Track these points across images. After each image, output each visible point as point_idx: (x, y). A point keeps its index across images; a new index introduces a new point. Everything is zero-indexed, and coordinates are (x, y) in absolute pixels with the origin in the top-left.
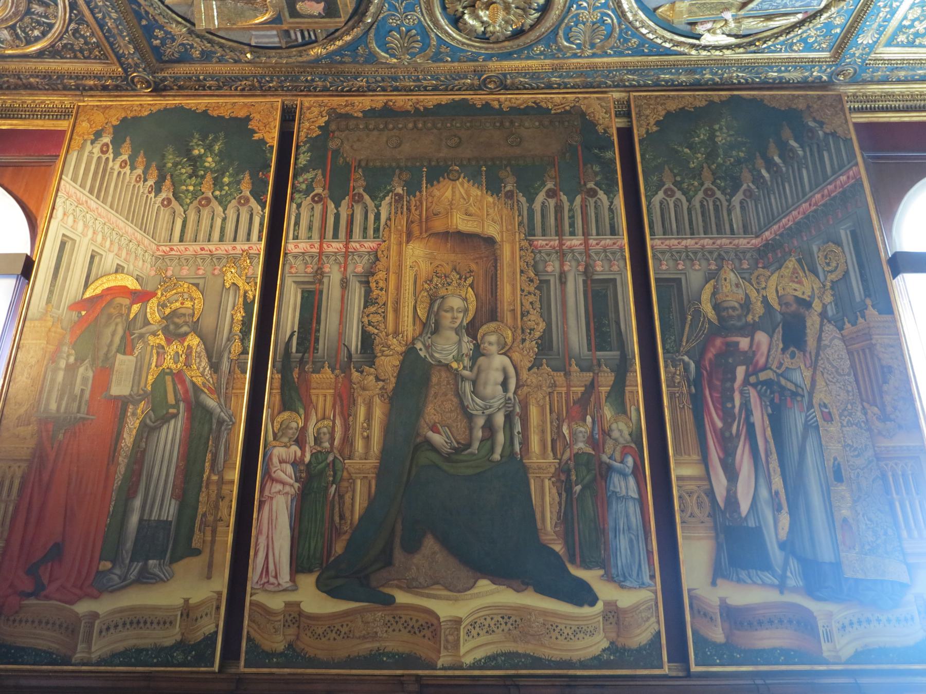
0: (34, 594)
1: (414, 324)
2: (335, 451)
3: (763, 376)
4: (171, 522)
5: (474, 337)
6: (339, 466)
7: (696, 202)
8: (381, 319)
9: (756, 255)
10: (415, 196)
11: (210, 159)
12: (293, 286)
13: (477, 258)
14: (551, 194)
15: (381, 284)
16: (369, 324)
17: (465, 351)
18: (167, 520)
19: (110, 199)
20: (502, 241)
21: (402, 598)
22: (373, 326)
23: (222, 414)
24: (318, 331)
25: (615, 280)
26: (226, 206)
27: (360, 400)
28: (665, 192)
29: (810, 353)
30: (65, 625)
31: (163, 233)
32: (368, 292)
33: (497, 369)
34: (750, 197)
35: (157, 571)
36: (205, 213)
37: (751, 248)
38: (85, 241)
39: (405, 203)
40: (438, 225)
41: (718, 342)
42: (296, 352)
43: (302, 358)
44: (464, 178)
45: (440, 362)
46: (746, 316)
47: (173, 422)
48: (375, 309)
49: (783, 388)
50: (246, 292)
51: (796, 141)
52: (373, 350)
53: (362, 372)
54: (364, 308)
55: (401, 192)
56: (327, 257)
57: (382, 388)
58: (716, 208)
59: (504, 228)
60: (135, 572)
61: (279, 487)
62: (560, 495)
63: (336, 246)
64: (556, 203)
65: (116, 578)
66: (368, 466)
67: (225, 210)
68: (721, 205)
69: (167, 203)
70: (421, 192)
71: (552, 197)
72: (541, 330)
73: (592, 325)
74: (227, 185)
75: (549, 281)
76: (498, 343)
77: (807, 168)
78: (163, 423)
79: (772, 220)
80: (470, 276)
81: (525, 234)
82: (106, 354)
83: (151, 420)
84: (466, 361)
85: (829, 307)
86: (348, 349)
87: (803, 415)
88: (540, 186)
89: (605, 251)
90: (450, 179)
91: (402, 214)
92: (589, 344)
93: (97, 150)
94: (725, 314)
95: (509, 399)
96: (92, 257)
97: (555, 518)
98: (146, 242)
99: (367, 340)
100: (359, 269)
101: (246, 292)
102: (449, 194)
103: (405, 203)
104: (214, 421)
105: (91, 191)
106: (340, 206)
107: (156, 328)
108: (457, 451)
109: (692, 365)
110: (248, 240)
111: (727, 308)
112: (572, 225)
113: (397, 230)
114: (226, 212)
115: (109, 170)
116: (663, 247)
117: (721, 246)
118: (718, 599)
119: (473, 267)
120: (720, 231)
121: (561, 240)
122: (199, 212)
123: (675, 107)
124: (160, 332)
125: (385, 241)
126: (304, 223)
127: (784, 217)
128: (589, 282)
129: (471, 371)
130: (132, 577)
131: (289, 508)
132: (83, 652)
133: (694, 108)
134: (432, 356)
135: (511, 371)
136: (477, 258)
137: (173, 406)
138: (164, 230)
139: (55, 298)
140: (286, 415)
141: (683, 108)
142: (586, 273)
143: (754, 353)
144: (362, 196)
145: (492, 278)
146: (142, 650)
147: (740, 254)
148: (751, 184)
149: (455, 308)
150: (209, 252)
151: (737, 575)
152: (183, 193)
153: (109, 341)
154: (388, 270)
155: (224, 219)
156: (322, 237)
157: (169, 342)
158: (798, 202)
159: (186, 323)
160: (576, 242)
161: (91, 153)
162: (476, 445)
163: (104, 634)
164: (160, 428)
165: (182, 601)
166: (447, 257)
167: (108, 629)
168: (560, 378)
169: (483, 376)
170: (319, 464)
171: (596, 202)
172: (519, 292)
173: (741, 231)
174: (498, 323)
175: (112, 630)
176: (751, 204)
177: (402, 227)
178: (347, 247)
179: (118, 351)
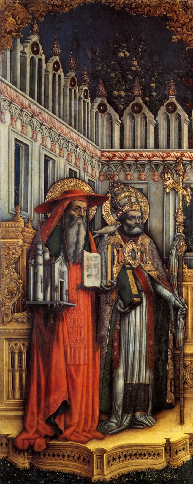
4: (148, 385)
11: (135, 63)
18: (145, 384)
23: (177, 302)
26: (157, 113)
30: (82, 457)
31: (105, 140)
35: (142, 419)
38: (37, 145)
47: (138, 308)
50: (184, 197)
60: (127, 421)
65: (114, 425)
67: (155, 115)
69: (102, 109)
78: (131, 309)
83: (121, 307)
93: (28, 50)
98: (91, 148)
104: (171, 307)
105: (32, 95)
107: (113, 229)
110: (180, 146)
114: (157, 119)
115: (44, 72)
122: (133, 118)
124: (117, 233)
132: (99, 475)
137: (137, 296)
138: (104, 136)
146: (140, 473)
150: (147, 159)
159: (137, 225)
161: (23, 52)
163: (111, 463)
164: (129, 313)
165: (164, 441)
167: (114, 459)
175: (117, 460)
179: (84, 248)
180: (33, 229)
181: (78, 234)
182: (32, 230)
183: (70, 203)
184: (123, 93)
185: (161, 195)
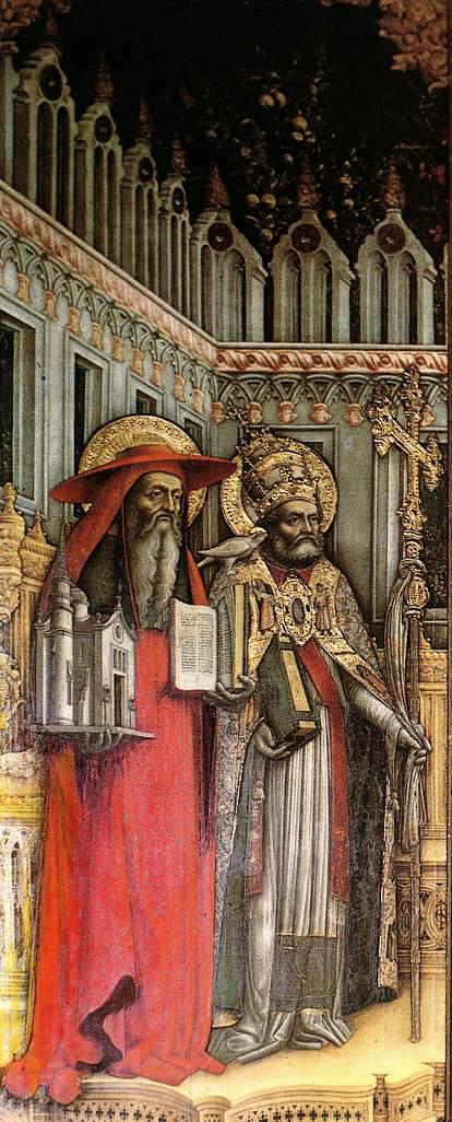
19: (90, 223)
31: (227, 319)
35: (320, 1027)
36: (311, 268)
38: (56, 331)
50: (421, 467)
65: (250, 1039)
67: (353, 259)
74: (350, 196)
78: (293, 749)
82: (152, 603)
83: (266, 741)
96: (80, 375)
104: (391, 746)
105: (43, 202)
110: (413, 337)
114: (357, 266)
115: (72, 144)
122: (297, 263)
124: (256, 555)
130: (280, 1039)
152: (254, 212)
153: (153, 572)
155: (355, 287)
157: (280, 578)
159: (307, 536)
165: (373, 1083)
179: (175, 594)
181: (159, 558)
182: (43, 545)
183: (138, 481)
184: (271, 201)
185: (369, 462)
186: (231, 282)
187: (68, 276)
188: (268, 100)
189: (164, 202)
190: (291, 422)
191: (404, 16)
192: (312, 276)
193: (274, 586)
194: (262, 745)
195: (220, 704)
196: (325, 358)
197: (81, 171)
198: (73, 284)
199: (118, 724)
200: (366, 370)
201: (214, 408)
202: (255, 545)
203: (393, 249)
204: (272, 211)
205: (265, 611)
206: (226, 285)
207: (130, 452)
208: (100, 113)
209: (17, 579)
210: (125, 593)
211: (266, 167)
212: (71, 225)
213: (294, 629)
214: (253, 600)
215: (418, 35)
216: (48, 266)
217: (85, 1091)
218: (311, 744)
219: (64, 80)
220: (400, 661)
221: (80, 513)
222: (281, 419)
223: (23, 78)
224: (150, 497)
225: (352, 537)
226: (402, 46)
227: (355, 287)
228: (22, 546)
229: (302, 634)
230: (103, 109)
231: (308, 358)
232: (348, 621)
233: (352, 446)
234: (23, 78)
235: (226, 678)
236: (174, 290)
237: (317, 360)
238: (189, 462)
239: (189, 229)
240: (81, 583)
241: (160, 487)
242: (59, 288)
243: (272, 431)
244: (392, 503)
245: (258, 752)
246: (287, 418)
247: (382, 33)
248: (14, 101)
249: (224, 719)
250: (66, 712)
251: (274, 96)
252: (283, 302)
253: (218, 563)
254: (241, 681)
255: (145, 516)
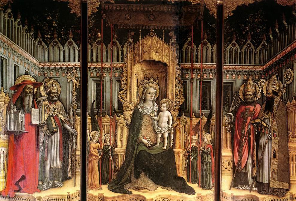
0: (18, 191)
1: (137, 99)
2: (111, 145)
3: (256, 121)
5: (159, 105)
6: (113, 150)
7: (243, 50)
8: (125, 96)
9: (262, 73)
10: (136, 43)
11: (54, 22)
12: (93, 82)
13: (160, 72)
14: (190, 44)
15: (125, 82)
16: (121, 98)
17: (155, 109)
20: (170, 65)
21: (134, 192)
22: (122, 99)
24: (103, 100)
25: (210, 82)
26: (64, 45)
27: (119, 127)
28: (232, 45)
29: (274, 112)
31: (41, 58)
32: (120, 85)
33: (166, 117)
34: (264, 48)
36: (56, 48)
37: (260, 70)
38: (11, 60)
39: (133, 46)
40: (146, 57)
41: (243, 108)
42: (96, 109)
43: (98, 111)
44: (156, 35)
45: (146, 113)
46: (254, 98)
48: (123, 92)
49: (262, 125)
50: (76, 84)
51: (286, 22)
52: (123, 108)
53: (119, 117)
54: (119, 92)
55: (131, 41)
56: (104, 70)
57: (126, 123)
58: (250, 52)
59: (170, 59)
61: (94, 157)
62: (186, 160)
63: (107, 65)
64: (191, 48)
66: (123, 150)
67: (64, 47)
68: (252, 51)
69: (40, 43)
70: (139, 41)
71: (190, 45)
72: (183, 102)
73: (201, 99)
75: (187, 81)
76: (167, 107)
77: (288, 35)
78: (53, 134)
79: (270, 58)
80: (158, 79)
81: (178, 62)
82: (28, 108)
83: (48, 133)
84: (156, 114)
85: (284, 95)
86: (114, 107)
87: (267, 135)
88: (185, 40)
89: (208, 69)
90: (150, 36)
91: (132, 51)
92: (199, 108)
94: (247, 97)
95: (170, 128)
96: (15, 67)
97: (184, 168)
99: (121, 104)
100: (117, 76)
101: (76, 84)
102: (150, 43)
103: (133, 46)
104: (70, 134)
106: (108, 47)
108: (152, 146)
109: (233, 116)
110: (74, 61)
111: (248, 95)
112: (197, 58)
113: (130, 59)
114: (64, 48)
115: (13, 26)
116: (228, 69)
117: (250, 69)
118: (231, 194)
119: (160, 76)
120: (250, 63)
121: (192, 64)
122: (54, 48)
123: (241, 4)
124: (46, 100)
125: (125, 63)
126: (94, 54)
127: (275, 57)
128: (201, 83)
129: (157, 117)
131: (98, 164)
133: (248, 4)
134: (144, 111)
135: (171, 118)
136: (160, 72)
139: (4, 84)
140: (94, 132)
141: (244, 4)
142: (200, 79)
143: (255, 112)
144: (116, 42)
145: (165, 80)
147: (255, 72)
148: (265, 42)
149: (152, 93)
151: (238, 186)
152: (46, 38)
154: (127, 77)
155: (64, 52)
156: (102, 61)
158: (281, 50)
159: (55, 96)
160: (198, 65)
162: (158, 144)
166: (150, 71)
168: (188, 120)
169: (161, 119)
170: (106, 149)
171: (206, 48)
172: (175, 86)
173: (258, 62)
174: (166, 99)
176: (264, 51)
177: (132, 57)
178: (111, 65)
179: (32, 107)
180: (9, 97)
181: (29, 100)
182: (8, 98)
183: (25, 86)
184: (49, 36)
185: (66, 83)
186: (42, 51)
187: (13, 50)
188: (48, 18)
189: (30, 37)
190: (53, 76)
191: (73, 3)
192: (56, 50)
193: (49, 105)
194: (47, 133)
195: (40, 126)
196: (59, 64)
197: (15, 31)
198: (14, 51)
199: (22, 130)
200: (66, 67)
201: (39, 73)
202: (46, 98)
203: (71, 45)
204: (49, 38)
205: (48, 110)
206: (41, 52)
207: (24, 81)
208: (18, 21)
209: (4, 104)
210: (23, 107)
211: (48, 30)
212: (13, 41)
213: (53, 113)
214: (46, 108)
215: (75, 7)
216: (9, 48)
217: (16, 195)
218: (56, 133)
219: (12, 15)
220: (72, 119)
221: (15, 92)
222: (51, 75)
223: (5, 15)
224: (27, 89)
225: (63, 96)
226: (72, 9)
227: (64, 52)
228: (5, 98)
229: (55, 114)
230: (19, 20)
231: (56, 65)
232: (63, 111)
233: (63, 80)
234: (5, 15)
235: (41, 122)
236: (32, 52)
237: (57, 65)
238: (34, 83)
239: (34, 41)
240: (15, 105)
241: (29, 88)
242: (11, 52)
243: (49, 77)
244: (71, 90)
245: (47, 135)
246: (52, 75)
247: (69, 6)
248: (3, 19)
249: (40, 129)
250: (12, 128)
251: (49, 18)
252: (51, 54)
253: (40, 101)
254: (44, 122)
255: (26, 93)
